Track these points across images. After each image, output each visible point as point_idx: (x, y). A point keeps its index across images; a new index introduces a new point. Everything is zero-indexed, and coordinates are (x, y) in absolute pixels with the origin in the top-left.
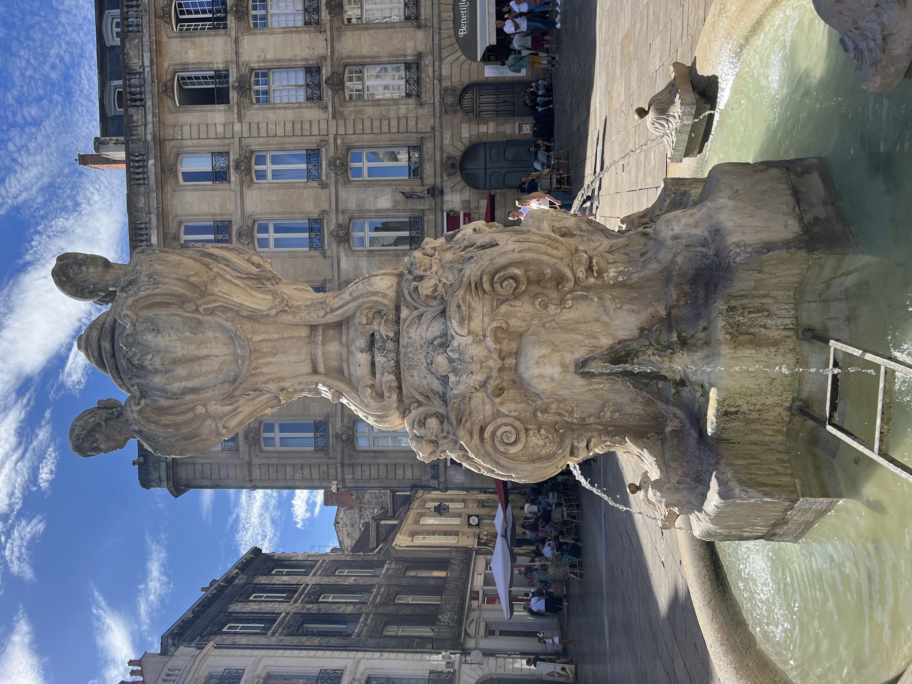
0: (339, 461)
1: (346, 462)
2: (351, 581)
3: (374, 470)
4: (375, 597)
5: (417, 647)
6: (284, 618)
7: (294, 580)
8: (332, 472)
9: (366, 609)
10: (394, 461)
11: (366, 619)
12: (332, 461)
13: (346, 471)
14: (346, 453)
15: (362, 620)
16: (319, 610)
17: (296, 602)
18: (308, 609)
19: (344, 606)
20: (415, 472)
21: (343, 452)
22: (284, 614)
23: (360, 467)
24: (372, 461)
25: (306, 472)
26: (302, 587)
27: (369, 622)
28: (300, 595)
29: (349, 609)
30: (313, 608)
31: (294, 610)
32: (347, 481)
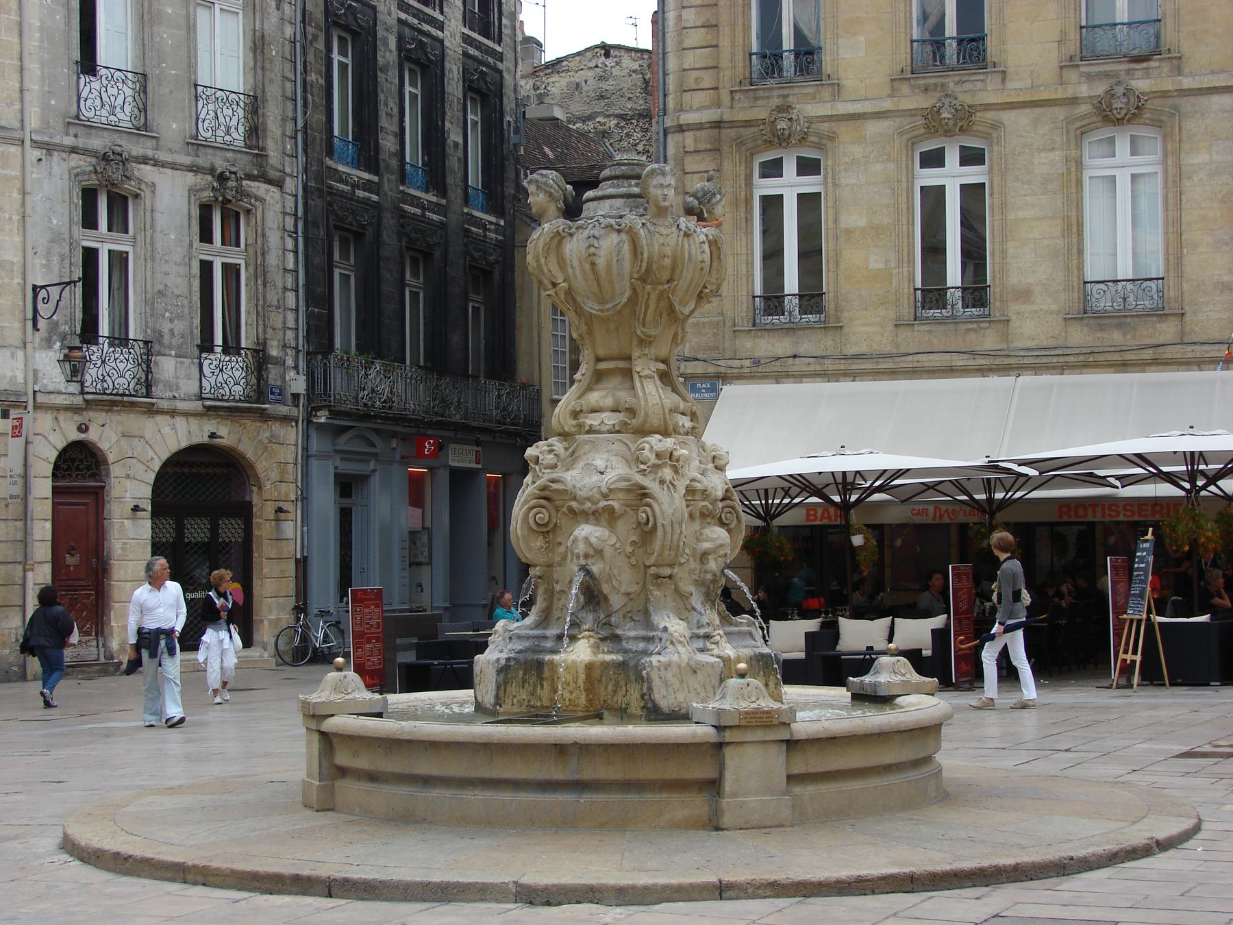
1: (724, 131)
2: (455, 136)
4: (415, 201)
5: (309, 316)
8: (699, 98)
9: (389, 182)
11: (367, 186)
13: (703, 134)
15: (366, 176)
16: (385, 70)
18: (386, 44)
19: (394, 128)
21: (747, 124)
26: (437, 15)
27: (361, 194)
28: (417, 14)
29: (388, 143)
30: (388, 53)
32: (678, 137)
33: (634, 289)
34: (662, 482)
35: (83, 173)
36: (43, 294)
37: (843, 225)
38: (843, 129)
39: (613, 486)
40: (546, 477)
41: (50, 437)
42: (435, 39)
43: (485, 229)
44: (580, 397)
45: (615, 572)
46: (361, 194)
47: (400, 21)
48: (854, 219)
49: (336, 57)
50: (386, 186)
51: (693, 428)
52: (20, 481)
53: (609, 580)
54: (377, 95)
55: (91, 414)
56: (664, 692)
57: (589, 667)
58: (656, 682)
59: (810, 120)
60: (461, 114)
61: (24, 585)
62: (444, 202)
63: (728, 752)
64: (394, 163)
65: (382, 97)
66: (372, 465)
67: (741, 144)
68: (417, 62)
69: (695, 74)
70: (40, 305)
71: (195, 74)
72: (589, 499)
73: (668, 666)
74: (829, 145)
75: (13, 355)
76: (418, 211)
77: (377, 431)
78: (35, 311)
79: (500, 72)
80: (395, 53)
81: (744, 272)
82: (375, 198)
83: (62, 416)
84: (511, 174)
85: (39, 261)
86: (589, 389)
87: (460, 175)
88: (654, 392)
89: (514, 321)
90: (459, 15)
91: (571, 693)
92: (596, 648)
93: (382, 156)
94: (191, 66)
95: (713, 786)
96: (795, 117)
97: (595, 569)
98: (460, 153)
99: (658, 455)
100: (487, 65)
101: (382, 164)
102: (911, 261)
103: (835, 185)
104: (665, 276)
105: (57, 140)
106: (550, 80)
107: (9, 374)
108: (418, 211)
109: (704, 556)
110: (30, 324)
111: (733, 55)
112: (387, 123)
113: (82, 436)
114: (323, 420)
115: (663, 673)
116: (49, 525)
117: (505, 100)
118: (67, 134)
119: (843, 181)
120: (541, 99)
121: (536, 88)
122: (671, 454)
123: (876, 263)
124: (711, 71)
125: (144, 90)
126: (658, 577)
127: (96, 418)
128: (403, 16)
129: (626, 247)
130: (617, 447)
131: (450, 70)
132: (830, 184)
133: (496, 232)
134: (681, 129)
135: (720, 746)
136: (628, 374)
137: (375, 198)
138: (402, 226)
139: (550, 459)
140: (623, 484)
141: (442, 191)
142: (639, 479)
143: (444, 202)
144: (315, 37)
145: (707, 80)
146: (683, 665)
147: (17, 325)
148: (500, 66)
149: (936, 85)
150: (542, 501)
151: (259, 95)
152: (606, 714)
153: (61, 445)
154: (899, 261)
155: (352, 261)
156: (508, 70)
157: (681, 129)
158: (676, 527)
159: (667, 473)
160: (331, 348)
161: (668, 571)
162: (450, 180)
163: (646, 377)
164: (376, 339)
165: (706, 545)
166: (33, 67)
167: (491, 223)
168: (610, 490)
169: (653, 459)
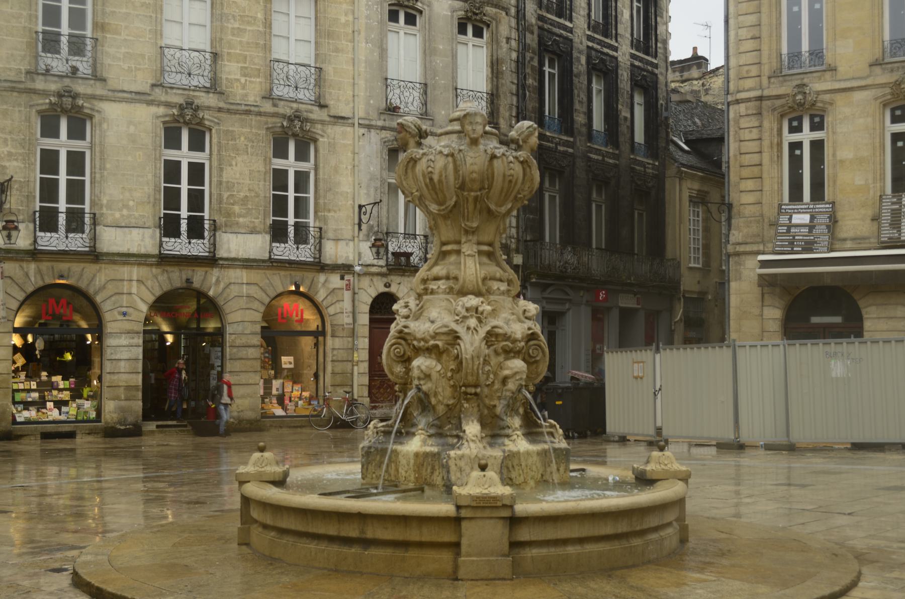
0: (766, 93)
3: (753, 146)
6: (565, 28)
7: (624, 28)
8: (749, 83)
9: (581, 143)
10: (765, 176)
11: (566, 144)
12: (765, 81)
14: (778, 102)
15: (565, 138)
16: (578, 76)
17: (590, 38)
18: (578, 60)
19: (585, 109)
20: (751, 207)
21: (778, 97)
22: (571, 25)
23: (757, 124)
24: (766, 143)
25: (749, 45)
26: (613, 43)
27: (561, 148)
28: (600, 43)
29: (580, 119)
30: (581, 64)
31: (576, 40)
32: (736, 107)
33: (457, 196)
34: (468, 328)
35: (389, 141)
36: (364, 209)
37: (838, 158)
38: (838, 97)
39: (437, 331)
40: (402, 324)
41: (370, 290)
42: (613, 57)
43: (645, 167)
44: (429, 270)
45: (440, 390)
46: (561, 148)
47: (588, 47)
48: (846, 153)
49: (547, 69)
50: (578, 143)
51: (509, 291)
52: (351, 315)
53: (436, 394)
54: (572, 90)
55: (392, 277)
56: (458, 475)
57: (417, 455)
58: (453, 468)
59: (818, 93)
60: (629, 101)
61: (352, 374)
62: (617, 152)
63: (464, 524)
64: (584, 130)
65: (576, 92)
66: (567, 306)
67: (774, 110)
68: (600, 71)
69: (746, 68)
70: (362, 216)
71: (456, 82)
72: (423, 339)
73: (461, 457)
74: (830, 108)
75: (347, 244)
76: (600, 158)
77: (571, 287)
78: (360, 219)
79: (656, 75)
80: (585, 66)
81: (776, 188)
82: (571, 150)
83: (375, 279)
84: (663, 134)
85: (363, 191)
86: (436, 264)
87: (628, 136)
88: (472, 266)
89: (664, 221)
90: (628, 42)
91: (406, 472)
92: (424, 442)
93: (576, 126)
94: (454, 78)
95: (457, 545)
96: (808, 92)
97: (424, 388)
98: (628, 123)
99: (467, 310)
100: (648, 71)
101: (575, 131)
102: (883, 179)
103: (834, 133)
104: (476, 186)
105: (373, 123)
106: (713, 80)
107: (345, 255)
108: (600, 158)
109: (505, 380)
110: (357, 227)
111: (770, 55)
112: (579, 107)
113: (386, 290)
114: (534, 280)
115: (458, 462)
116: (367, 340)
117: (659, 91)
118: (380, 119)
119: (839, 130)
120: (707, 91)
121: (703, 85)
122: (477, 309)
123: (859, 181)
124: (756, 66)
125: (425, 93)
126: (466, 393)
127: (395, 279)
128: (590, 44)
129: (451, 166)
130: (444, 304)
131: (622, 75)
132: (830, 133)
133: (653, 169)
134: (738, 102)
135: (456, 521)
136: (458, 252)
137: (571, 150)
138: (589, 166)
139: (404, 311)
140: (444, 330)
141: (616, 145)
142: (454, 326)
143: (617, 152)
144: (532, 59)
145: (754, 71)
146: (473, 457)
147: (350, 227)
148: (656, 71)
149: (898, 68)
150: (399, 340)
151: (495, 92)
152: (426, 488)
153: (374, 295)
154: (874, 179)
155: (557, 187)
156: (661, 74)
157: (738, 102)
158: (475, 359)
159: (473, 322)
160: (542, 237)
161: (473, 390)
162: (621, 139)
163: (469, 255)
164: (574, 234)
165: (507, 372)
166: (361, 83)
167: (649, 164)
168: (437, 334)
169: (464, 313)
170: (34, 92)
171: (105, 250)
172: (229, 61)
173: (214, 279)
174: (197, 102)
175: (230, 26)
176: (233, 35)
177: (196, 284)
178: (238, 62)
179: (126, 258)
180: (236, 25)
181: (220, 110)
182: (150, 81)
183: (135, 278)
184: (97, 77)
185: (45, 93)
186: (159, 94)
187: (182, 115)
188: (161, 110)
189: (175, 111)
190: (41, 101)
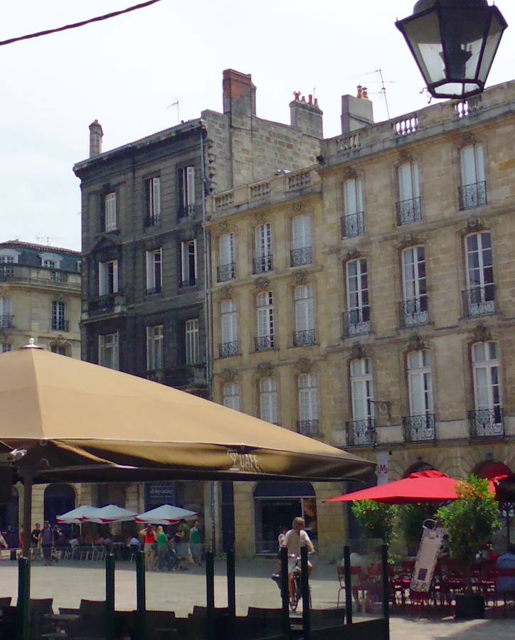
170: (400, 341)
171: (441, 438)
172: (504, 288)
173: (506, 452)
174: (485, 324)
175: (502, 263)
176: (505, 269)
177: (496, 458)
178: (509, 288)
179: (452, 442)
180: (506, 261)
181: (500, 326)
182: (458, 317)
183: (459, 455)
184: (431, 323)
185: (403, 341)
186: (464, 326)
187: (476, 336)
188: (466, 335)
189: (473, 335)
190: (403, 346)
